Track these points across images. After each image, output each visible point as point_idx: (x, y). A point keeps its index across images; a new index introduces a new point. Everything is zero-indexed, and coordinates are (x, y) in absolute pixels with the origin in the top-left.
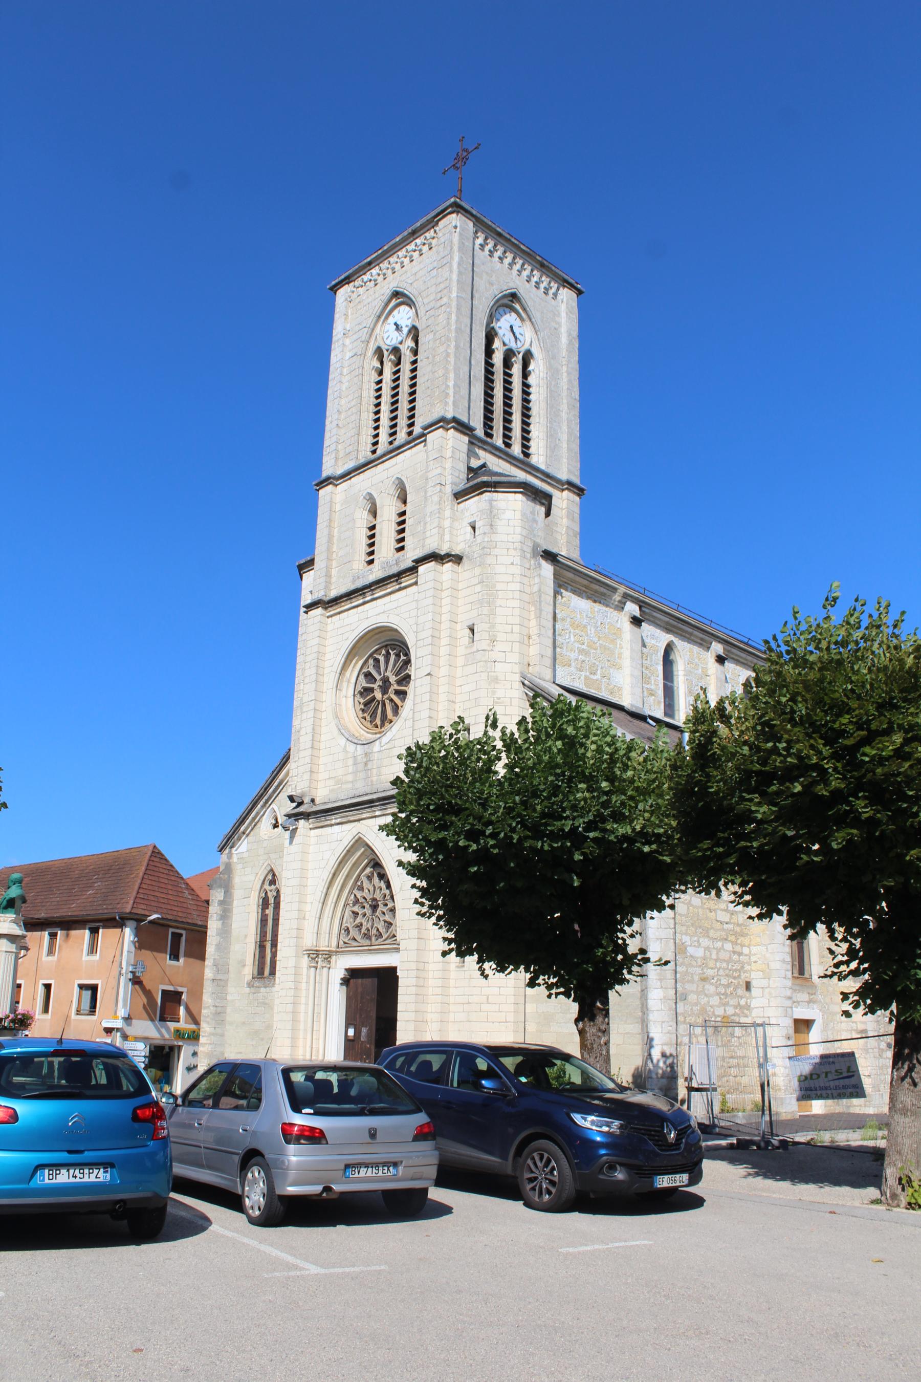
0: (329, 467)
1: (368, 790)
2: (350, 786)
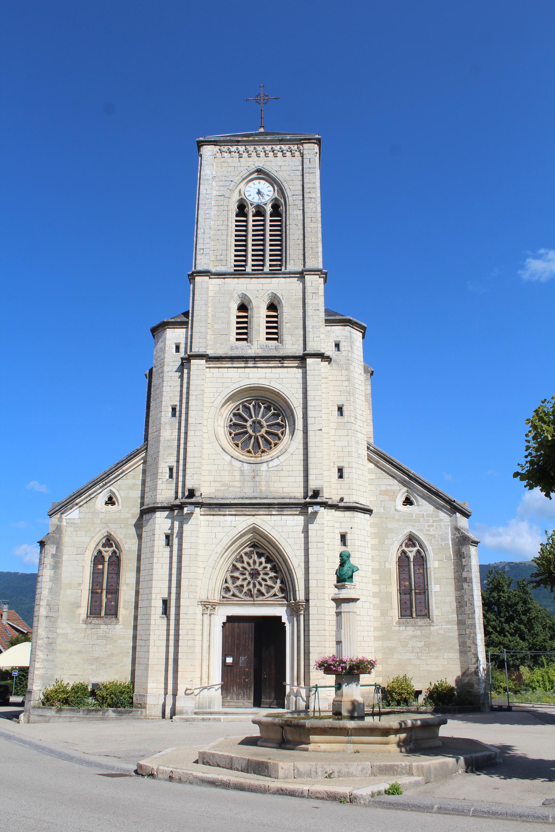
0: (202, 264)
1: (257, 495)
2: (238, 490)
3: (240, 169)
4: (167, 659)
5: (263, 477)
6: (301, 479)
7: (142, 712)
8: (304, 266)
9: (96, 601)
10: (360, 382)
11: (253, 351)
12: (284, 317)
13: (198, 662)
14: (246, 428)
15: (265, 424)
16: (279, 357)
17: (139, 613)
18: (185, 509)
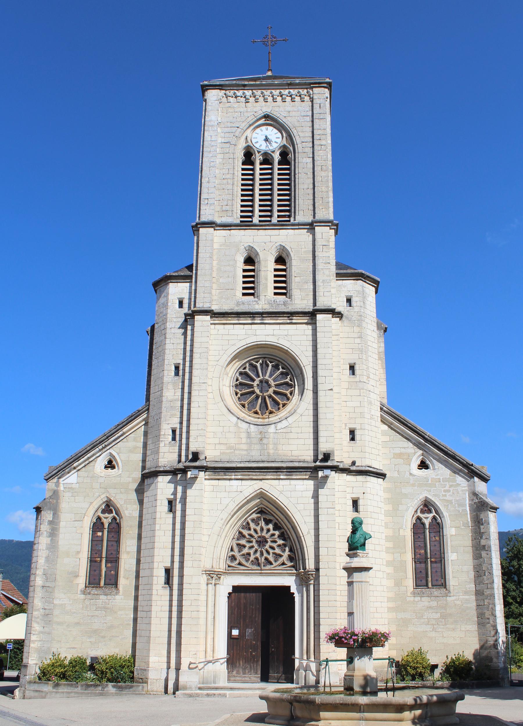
0: (207, 213)
1: (264, 458)
2: (245, 453)
3: (246, 115)
4: (170, 631)
5: (271, 439)
6: (311, 442)
7: (143, 687)
8: (314, 217)
9: (95, 571)
10: (373, 340)
11: (260, 307)
12: (293, 271)
13: (202, 635)
14: (253, 388)
15: (273, 383)
17: (140, 583)
18: (189, 473)
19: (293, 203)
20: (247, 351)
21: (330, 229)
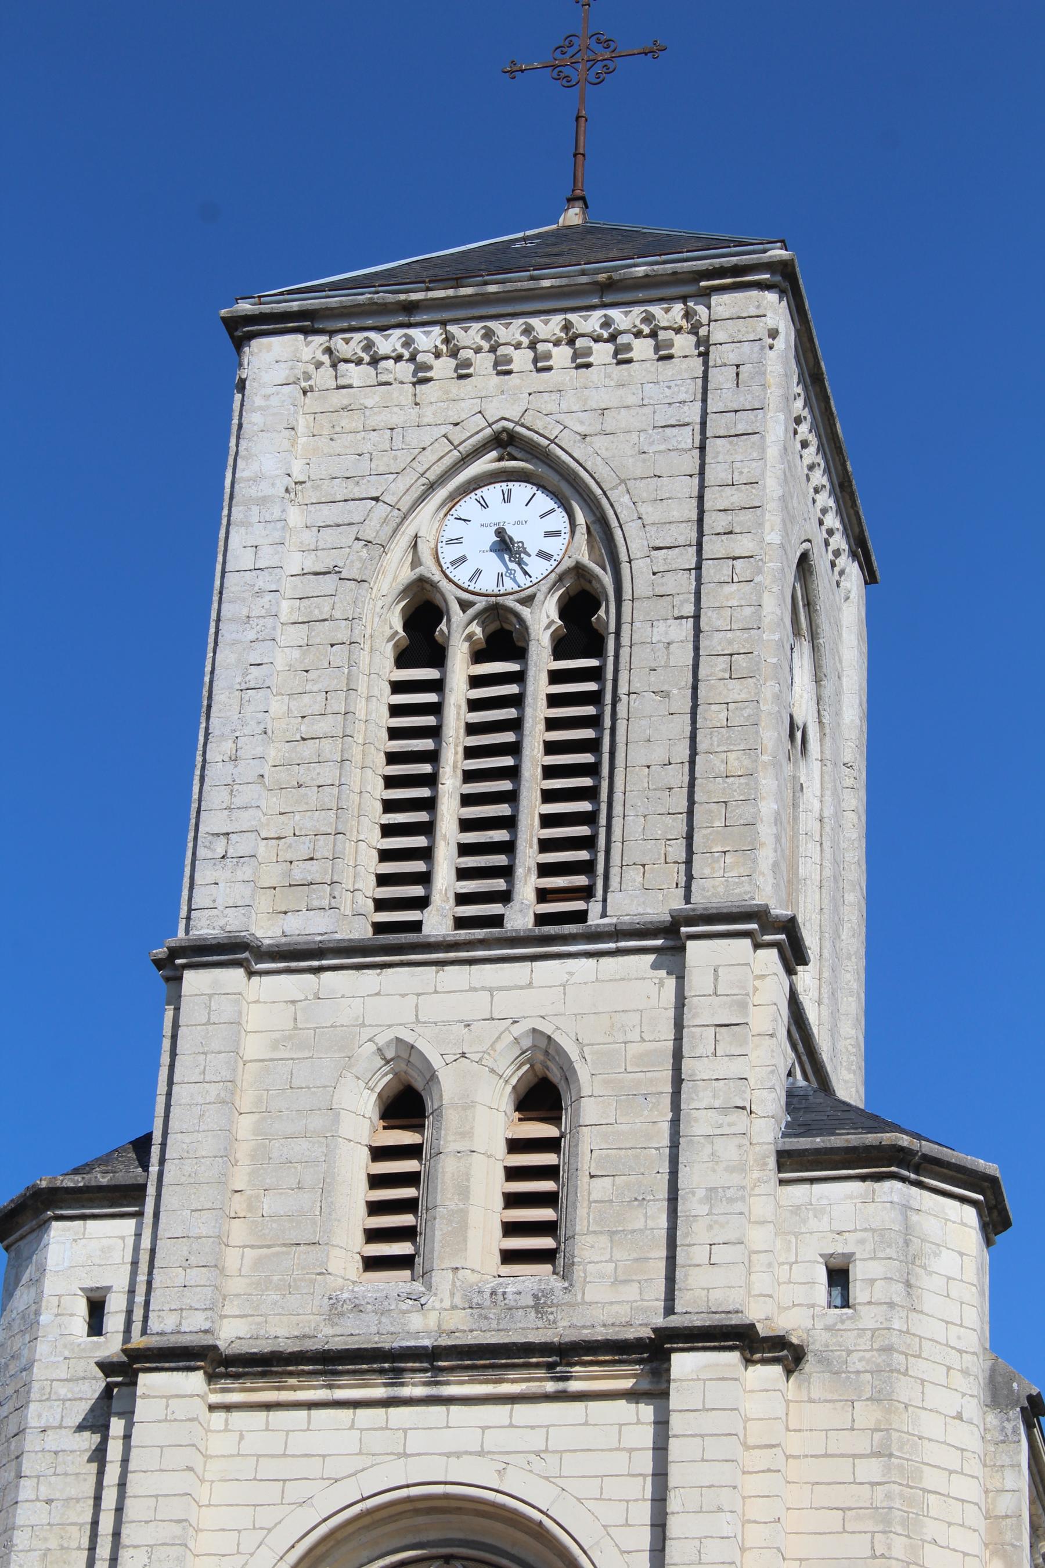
8: (687, 899)
11: (431, 1320)
12: (584, 1148)
16: (545, 1349)
19: (602, 832)
20: (367, 1528)
21: (757, 946)
